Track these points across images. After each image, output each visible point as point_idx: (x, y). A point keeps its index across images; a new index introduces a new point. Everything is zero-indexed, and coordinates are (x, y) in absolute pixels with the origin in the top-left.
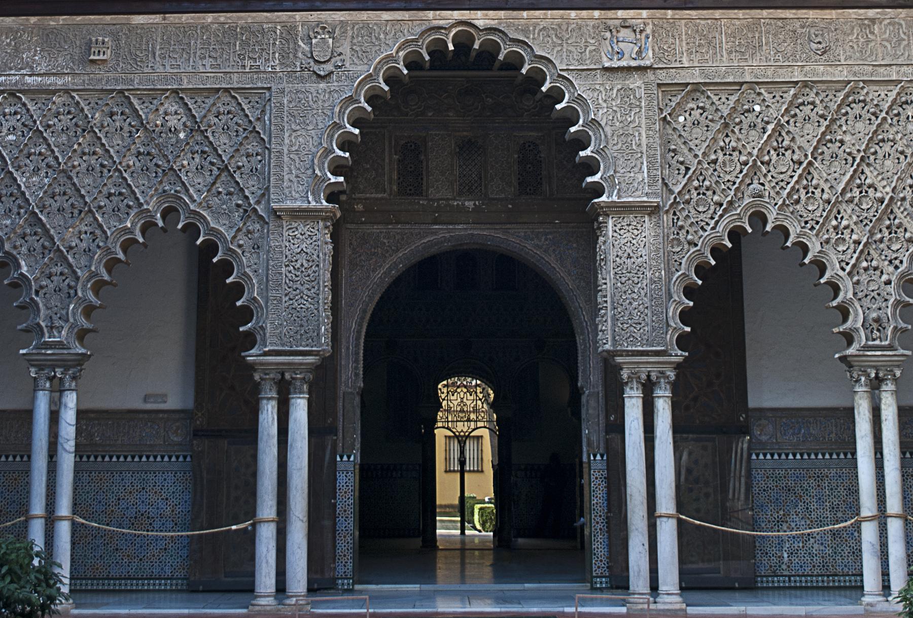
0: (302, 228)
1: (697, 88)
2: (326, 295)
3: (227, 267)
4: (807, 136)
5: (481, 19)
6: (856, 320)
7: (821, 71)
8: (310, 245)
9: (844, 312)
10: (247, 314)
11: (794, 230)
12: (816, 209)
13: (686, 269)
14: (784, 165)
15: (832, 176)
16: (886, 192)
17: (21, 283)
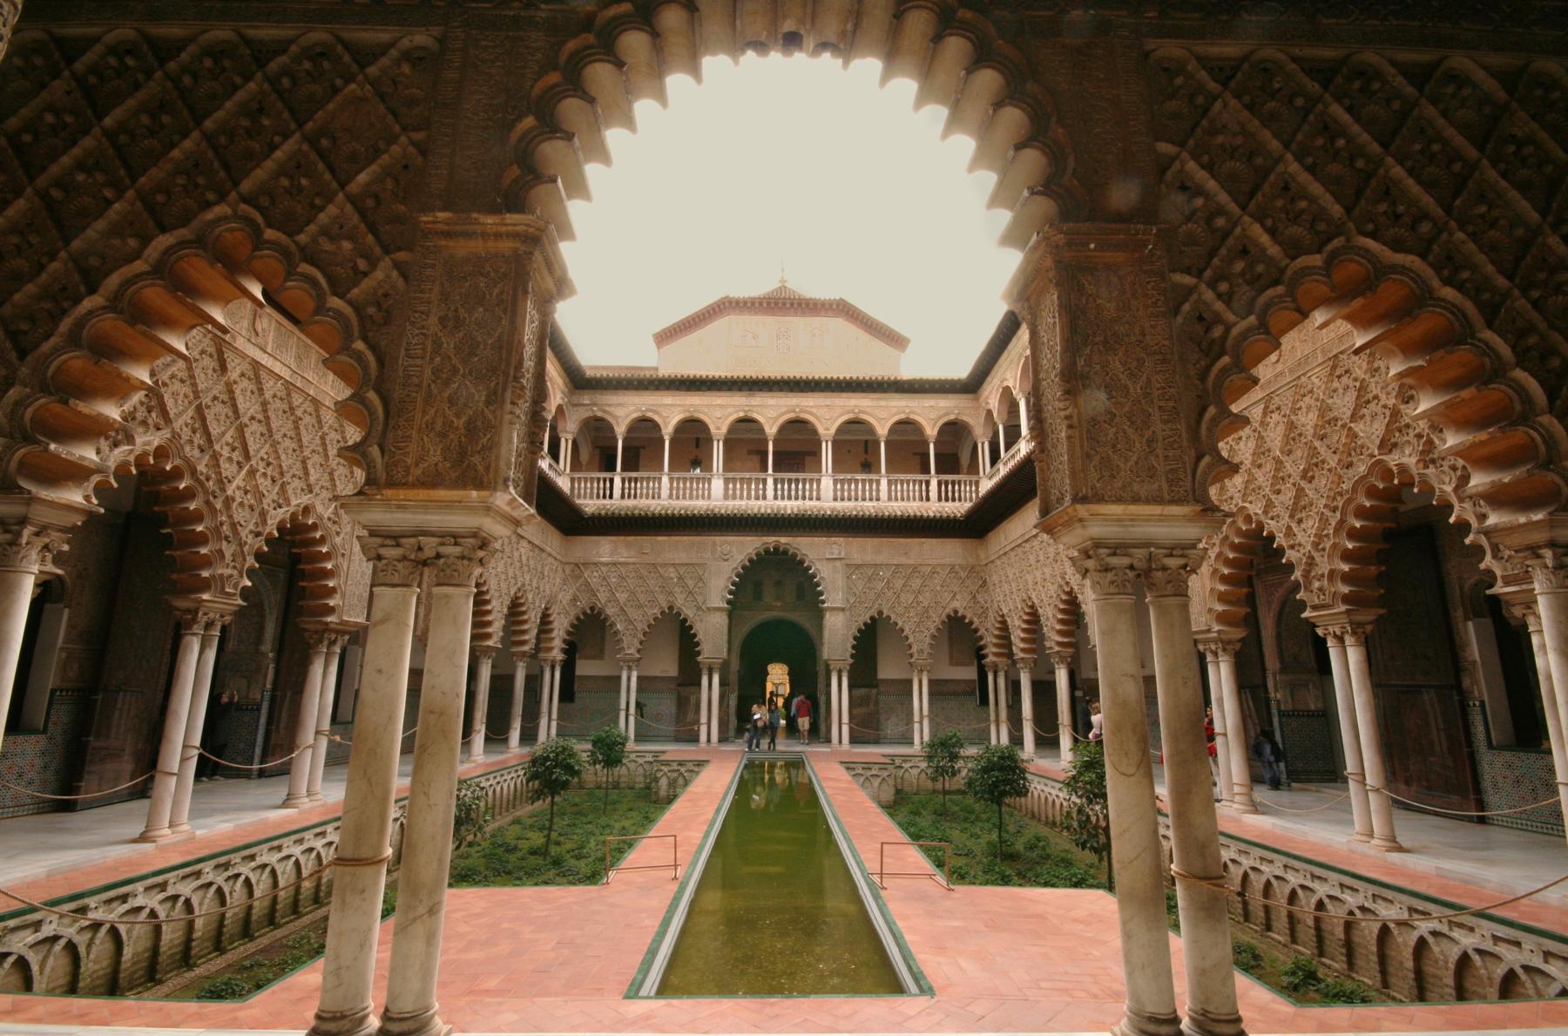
0: (718, 614)
1: (858, 566)
2: (726, 638)
3: (691, 627)
4: (899, 583)
5: (783, 540)
6: (914, 649)
7: (904, 560)
8: (720, 621)
9: (910, 646)
10: (698, 644)
11: (893, 617)
12: (900, 610)
13: (854, 631)
14: (890, 594)
15: (907, 598)
16: (926, 604)
17: (617, 632)
